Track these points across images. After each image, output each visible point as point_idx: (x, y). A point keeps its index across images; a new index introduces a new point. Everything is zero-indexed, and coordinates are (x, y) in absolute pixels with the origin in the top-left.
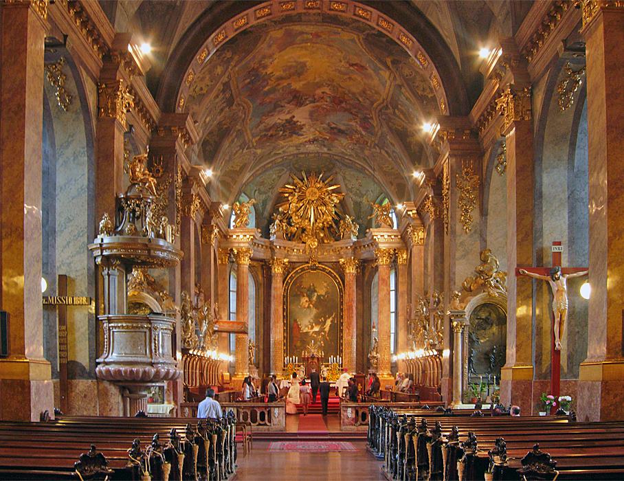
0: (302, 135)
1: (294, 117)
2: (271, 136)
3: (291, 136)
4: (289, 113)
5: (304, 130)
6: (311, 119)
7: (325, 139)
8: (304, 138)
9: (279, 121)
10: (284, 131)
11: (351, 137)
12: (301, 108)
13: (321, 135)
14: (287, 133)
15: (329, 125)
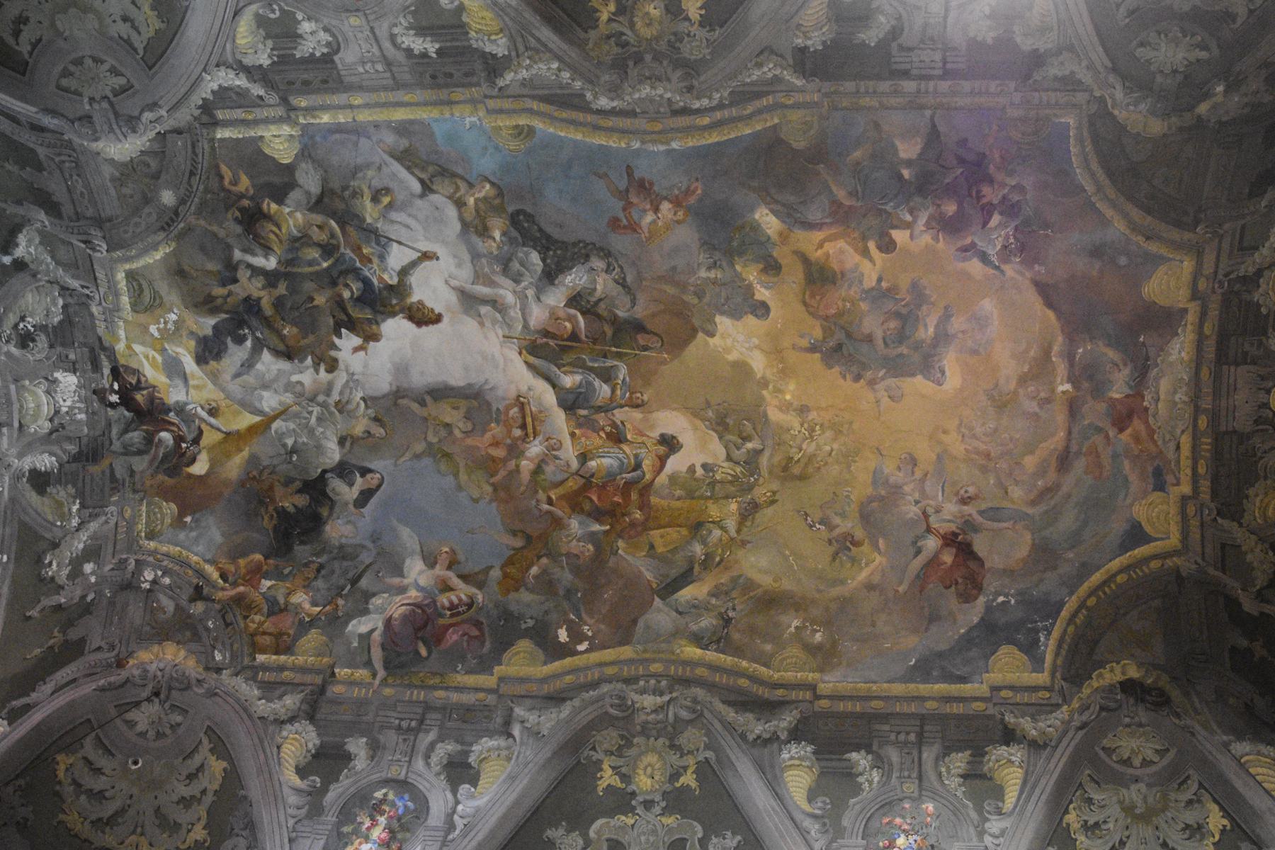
0: (208, 351)
1: (423, 317)
2: (252, 220)
3: (207, 304)
4: (469, 301)
5: (268, 363)
6: (398, 394)
7: (177, 460)
8: (173, 368)
9: (398, 257)
10: (271, 278)
11: (256, 573)
12: (513, 354)
13: (209, 438)
14: (249, 286)
15: (344, 470)
